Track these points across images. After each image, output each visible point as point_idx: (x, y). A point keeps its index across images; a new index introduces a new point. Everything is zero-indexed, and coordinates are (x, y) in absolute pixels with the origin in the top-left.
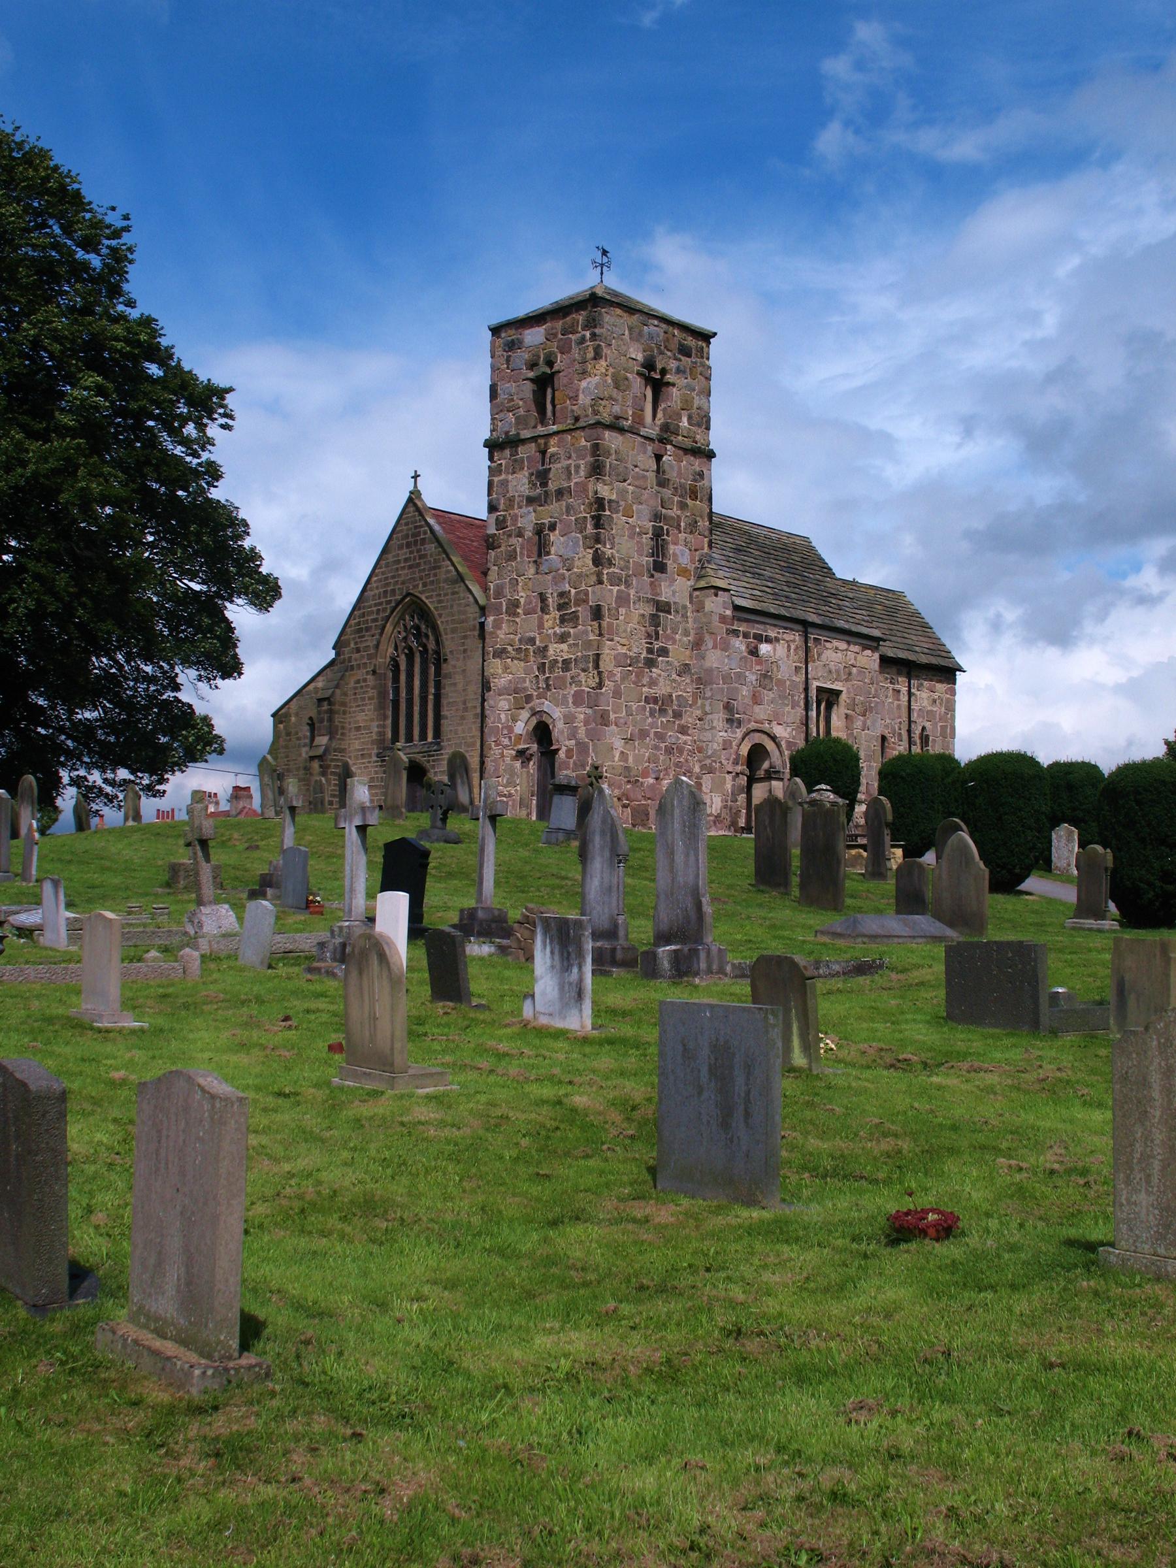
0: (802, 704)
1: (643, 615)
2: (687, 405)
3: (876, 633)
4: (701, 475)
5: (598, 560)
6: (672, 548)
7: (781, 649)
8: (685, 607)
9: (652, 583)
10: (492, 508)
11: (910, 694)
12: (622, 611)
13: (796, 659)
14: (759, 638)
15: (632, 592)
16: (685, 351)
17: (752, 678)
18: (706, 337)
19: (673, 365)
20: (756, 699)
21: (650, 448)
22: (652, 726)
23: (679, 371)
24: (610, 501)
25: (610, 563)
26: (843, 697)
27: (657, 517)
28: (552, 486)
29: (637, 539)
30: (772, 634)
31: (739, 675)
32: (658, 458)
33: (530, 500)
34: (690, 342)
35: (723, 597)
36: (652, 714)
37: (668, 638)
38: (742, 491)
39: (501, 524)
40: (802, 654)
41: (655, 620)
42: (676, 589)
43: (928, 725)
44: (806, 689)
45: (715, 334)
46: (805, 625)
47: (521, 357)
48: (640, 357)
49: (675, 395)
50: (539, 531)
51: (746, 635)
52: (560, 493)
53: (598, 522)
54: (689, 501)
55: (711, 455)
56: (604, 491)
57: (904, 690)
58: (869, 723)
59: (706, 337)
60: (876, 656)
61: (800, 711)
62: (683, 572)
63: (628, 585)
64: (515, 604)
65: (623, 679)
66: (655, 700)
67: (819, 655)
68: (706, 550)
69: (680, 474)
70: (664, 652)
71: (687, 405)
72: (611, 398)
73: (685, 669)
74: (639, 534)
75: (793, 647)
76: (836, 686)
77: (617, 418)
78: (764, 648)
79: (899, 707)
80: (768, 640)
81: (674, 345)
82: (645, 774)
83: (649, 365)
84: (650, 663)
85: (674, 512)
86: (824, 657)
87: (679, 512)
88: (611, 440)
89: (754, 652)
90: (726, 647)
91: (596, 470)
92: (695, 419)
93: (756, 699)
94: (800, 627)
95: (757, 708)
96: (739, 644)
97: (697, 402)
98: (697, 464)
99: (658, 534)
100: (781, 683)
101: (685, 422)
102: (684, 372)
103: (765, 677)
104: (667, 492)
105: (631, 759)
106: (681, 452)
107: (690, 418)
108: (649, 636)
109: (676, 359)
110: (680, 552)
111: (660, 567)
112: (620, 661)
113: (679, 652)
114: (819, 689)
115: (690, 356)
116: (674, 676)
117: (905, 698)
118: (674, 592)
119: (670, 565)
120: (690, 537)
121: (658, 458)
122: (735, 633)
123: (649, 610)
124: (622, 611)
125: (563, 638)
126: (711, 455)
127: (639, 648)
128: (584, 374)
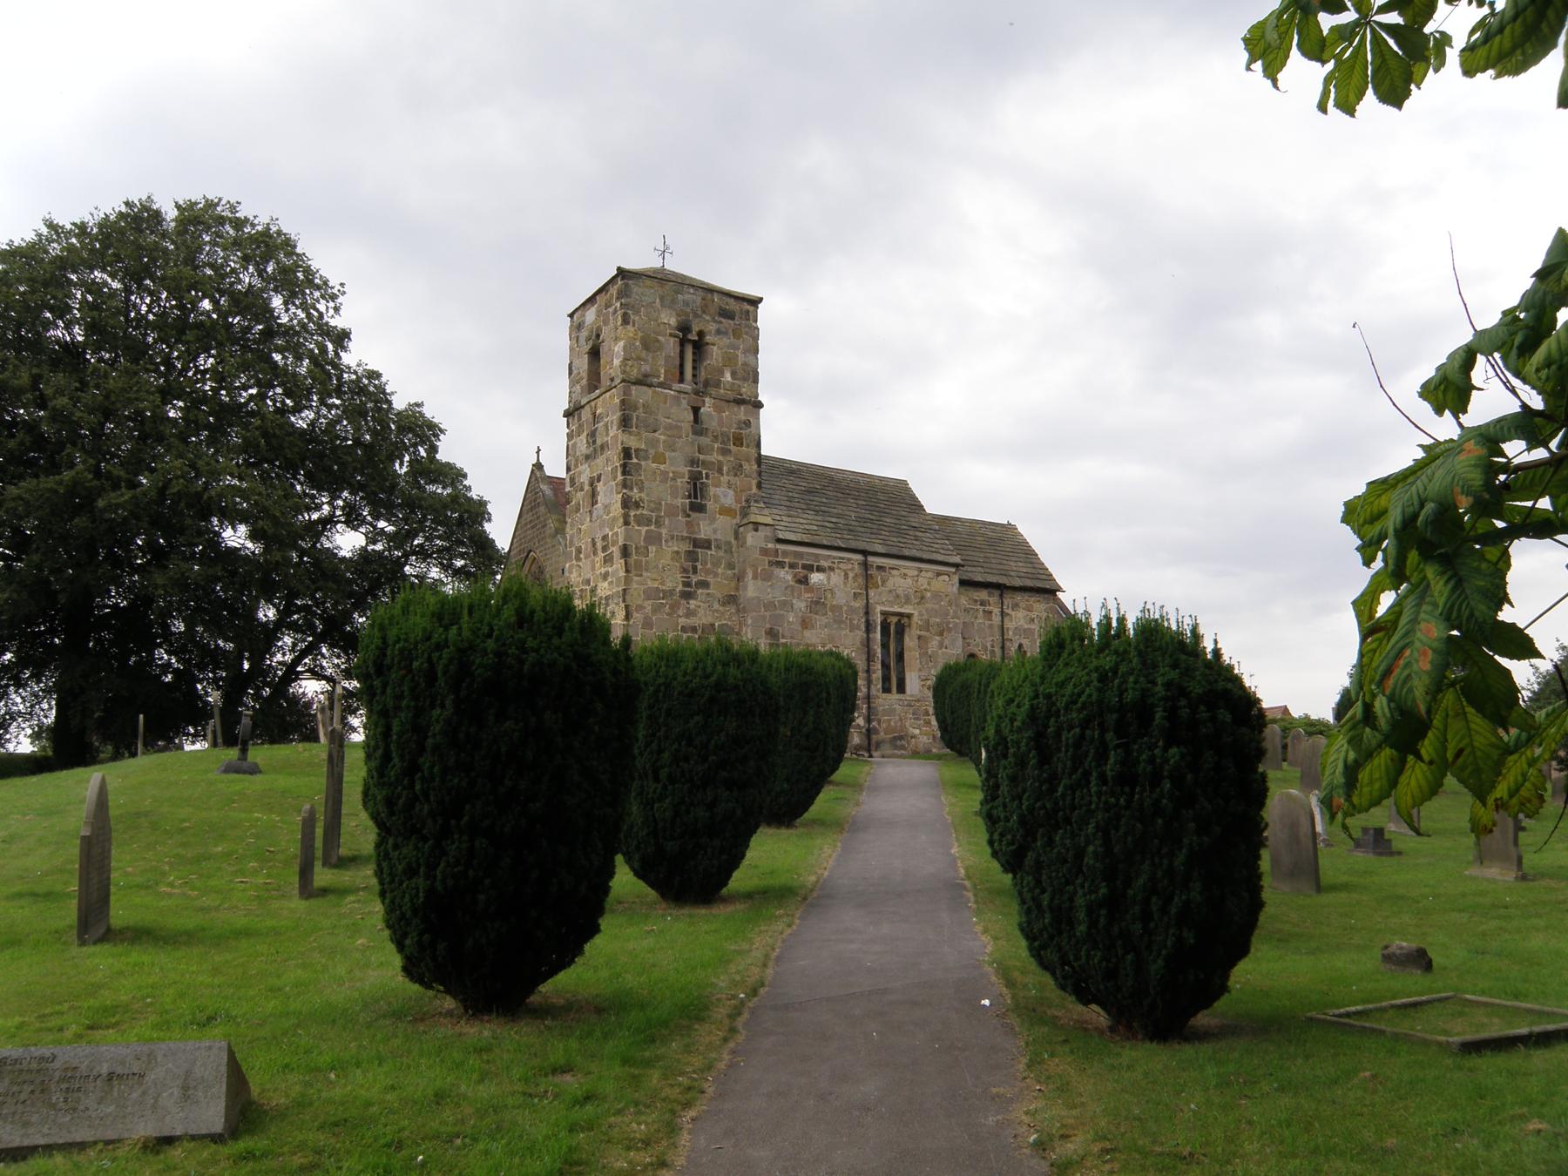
0: (863, 627)
1: (677, 553)
2: (730, 360)
3: (957, 559)
4: (747, 424)
5: (626, 503)
6: (712, 490)
7: (836, 578)
8: (729, 543)
9: (688, 523)
10: (568, 469)
11: (1002, 612)
12: (652, 549)
13: (853, 587)
14: (810, 568)
15: (664, 531)
16: (729, 315)
17: (800, 605)
18: (755, 302)
19: (712, 327)
20: (805, 624)
21: (684, 402)
23: (718, 332)
24: (637, 450)
25: (637, 505)
26: (915, 619)
27: (693, 462)
28: (599, 442)
29: (670, 483)
30: (825, 564)
31: (784, 603)
32: (696, 410)
33: (587, 457)
34: (746, 306)
35: (763, 532)
37: (708, 572)
38: (785, 433)
39: (572, 480)
40: (861, 580)
41: (692, 556)
42: (713, 527)
43: (1025, 642)
44: (867, 613)
45: (761, 300)
46: (865, 553)
47: (584, 334)
48: (673, 321)
49: (715, 354)
50: (593, 482)
51: (792, 566)
52: (602, 447)
53: (625, 470)
54: (732, 447)
55: (759, 405)
56: (633, 443)
57: (997, 611)
58: (946, 642)
59: (755, 302)
60: (956, 579)
61: (861, 634)
62: (726, 511)
63: (659, 524)
64: (579, 551)
65: (655, 611)
67: (884, 582)
68: (754, 490)
69: (721, 423)
70: (704, 584)
71: (730, 360)
72: (639, 358)
73: (731, 600)
74: (673, 479)
75: (851, 575)
77: (646, 376)
78: (816, 578)
79: (991, 626)
80: (820, 569)
83: (684, 328)
84: (687, 596)
85: (715, 457)
86: (890, 583)
88: (641, 395)
89: (804, 581)
90: (767, 577)
91: (625, 423)
92: (740, 374)
93: (805, 624)
94: (859, 557)
95: (807, 633)
96: (785, 575)
97: (741, 358)
98: (742, 413)
99: (695, 479)
100: (834, 608)
101: (728, 377)
102: (726, 333)
103: (817, 605)
104: (705, 440)
106: (724, 404)
107: (733, 374)
108: (685, 570)
110: (722, 494)
111: (698, 508)
112: (650, 594)
113: (720, 583)
114: (883, 613)
115: (733, 319)
116: (716, 606)
117: (996, 619)
118: (715, 531)
119: (710, 505)
120: (733, 480)
121: (696, 410)
122: (781, 564)
123: (686, 547)
124: (652, 549)
125: (605, 576)
126: (759, 405)
127: (674, 582)
128: (616, 339)
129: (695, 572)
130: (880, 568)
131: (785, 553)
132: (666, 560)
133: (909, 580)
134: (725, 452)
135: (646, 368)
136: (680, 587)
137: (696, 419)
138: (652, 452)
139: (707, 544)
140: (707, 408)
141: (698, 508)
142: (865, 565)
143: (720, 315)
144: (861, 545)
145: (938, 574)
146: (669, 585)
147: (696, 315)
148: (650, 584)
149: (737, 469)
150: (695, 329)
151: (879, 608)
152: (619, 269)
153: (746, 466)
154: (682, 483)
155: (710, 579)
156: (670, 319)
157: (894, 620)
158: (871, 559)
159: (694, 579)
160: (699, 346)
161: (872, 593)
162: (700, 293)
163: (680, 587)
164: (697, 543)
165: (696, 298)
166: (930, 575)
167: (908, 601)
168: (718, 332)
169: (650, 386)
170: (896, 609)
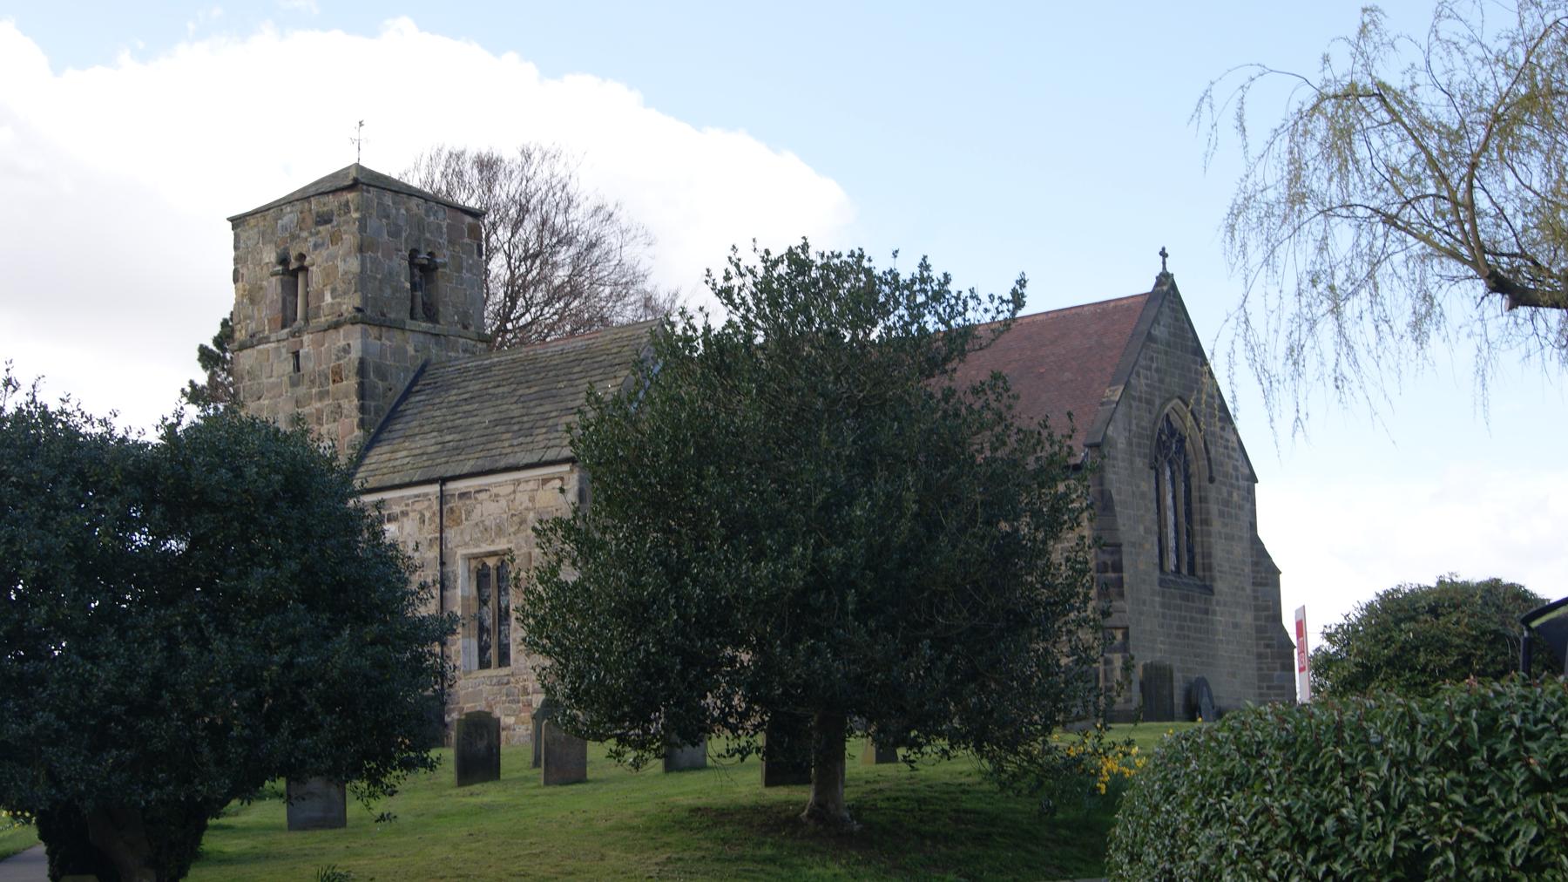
23: (316, 246)
30: (396, 509)
44: (442, 564)
46: (443, 481)
54: (331, 387)
67: (469, 513)
75: (427, 515)
76: (502, 545)
81: (309, 221)
83: (283, 260)
86: (476, 516)
87: (318, 405)
94: (436, 488)
101: (328, 298)
104: (301, 390)
107: (333, 291)
109: (311, 234)
114: (470, 558)
115: (329, 221)
121: (296, 355)
130: (463, 495)
133: (503, 502)
134: (322, 396)
137: (297, 368)
142: (443, 498)
143: (318, 223)
144: (441, 471)
145: (545, 481)
147: (294, 237)
149: (338, 412)
150: (293, 254)
151: (461, 552)
152: (237, 222)
153: (345, 403)
156: (270, 256)
157: (491, 562)
158: (452, 486)
161: (450, 534)
162: (298, 206)
165: (290, 217)
166: (532, 485)
167: (500, 531)
168: (316, 246)
169: (252, 346)
170: (486, 548)
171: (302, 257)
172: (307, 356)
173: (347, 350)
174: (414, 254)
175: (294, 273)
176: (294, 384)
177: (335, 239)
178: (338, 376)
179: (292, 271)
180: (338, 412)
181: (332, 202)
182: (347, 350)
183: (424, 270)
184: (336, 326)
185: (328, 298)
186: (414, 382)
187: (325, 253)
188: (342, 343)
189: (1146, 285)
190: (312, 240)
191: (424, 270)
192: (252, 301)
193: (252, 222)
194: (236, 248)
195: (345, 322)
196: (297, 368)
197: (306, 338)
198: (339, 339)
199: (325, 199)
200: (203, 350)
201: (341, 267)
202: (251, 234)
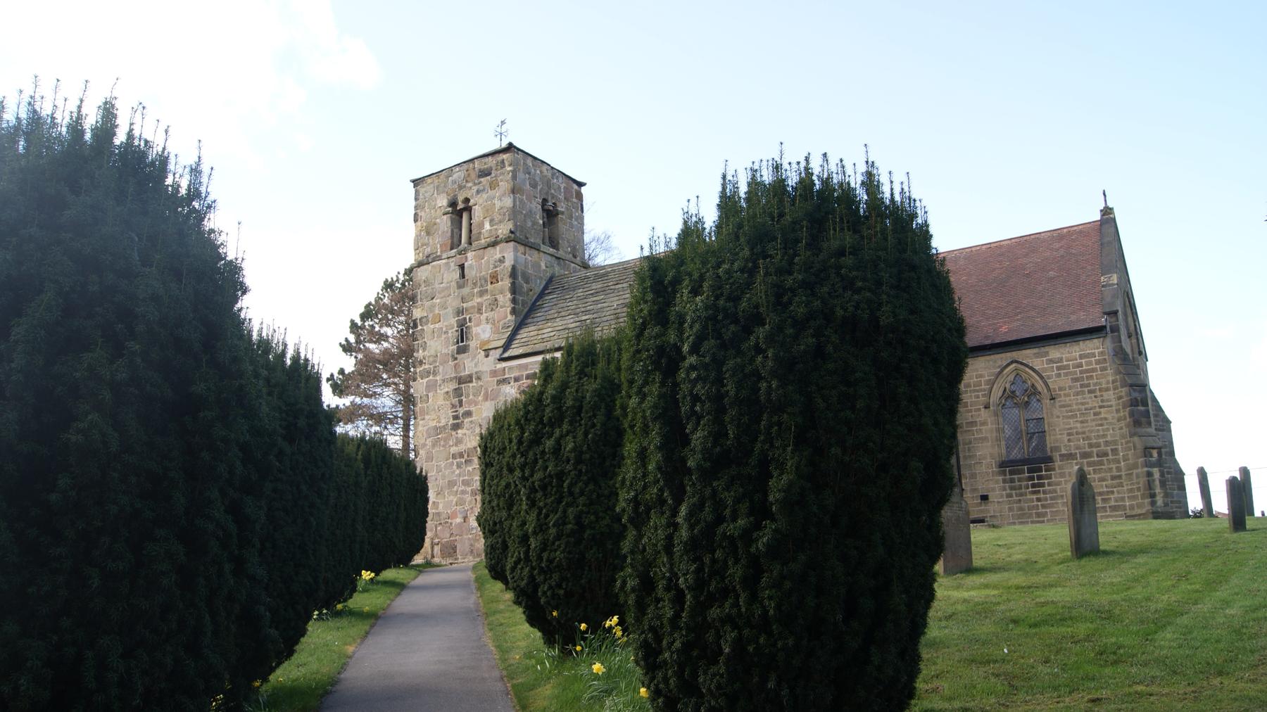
6: (475, 330)
22: (459, 475)
23: (478, 192)
36: (459, 466)
37: (470, 403)
41: (458, 392)
49: (477, 212)
51: (516, 380)
54: (489, 287)
66: (461, 455)
70: (468, 414)
81: (473, 175)
82: (454, 515)
83: (453, 204)
84: (456, 427)
87: (479, 300)
101: (487, 226)
104: (466, 291)
105: (441, 506)
107: (491, 221)
108: (453, 406)
109: (475, 184)
115: (489, 174)
119: (473, 344)
120: (490, 314)
121: (462, 267)
122: (504, 381)
123: (453, 386)
127: (446, 418)
129: (461, 402)
131: (511, 368)
132: (440, 402)
134: (481, 294)
135: (428, 250)
136: (451, 421)
137: (463, 276)
138: (431, 316)
139: (469, 379)
140: (471, 259)
141: (462, 350)
143: (480, 176)
146: (443, 422)
147: (461, 187)
148: (433, 424)
149: (494, 304)
150: (460, 199)
153: (500, 298)
154: (453, 333)
155: (473, 409)
156: (443, 202)
159: (461, 411)
160: (468, 209)
162: (465, 166)
163: (451, 421)
164: (461, 381)
165: (458, 175)
168: (478, 192)
171: (467, 200)
172: (471, 267)
173: (502, 260)
174: (545, 201)
175: (459, 214)
176: (460, 286)
177: (493, 186)
178: (494, 278)
179: (459, 211)
180: (494, 304)
181: (491, 161)
182: (502, 260)
183: (550, 214)
184: (494, 244)
185: (487, 226)
186: (546, 288)
187: (485, 196)
188: (498, 256)
189: (1093, 215)
190: (475, 188)
191: (550, 214)
192: (428, 233)
193: (429, 181)
194: (416, 199)
195: (501, 241)
196: (463, 276)
197: (470, 255)
198: (497, 253)
199: (486, 160)
200: (352, 322)
201: (498, 204)
202: (426, 189)
